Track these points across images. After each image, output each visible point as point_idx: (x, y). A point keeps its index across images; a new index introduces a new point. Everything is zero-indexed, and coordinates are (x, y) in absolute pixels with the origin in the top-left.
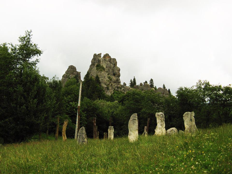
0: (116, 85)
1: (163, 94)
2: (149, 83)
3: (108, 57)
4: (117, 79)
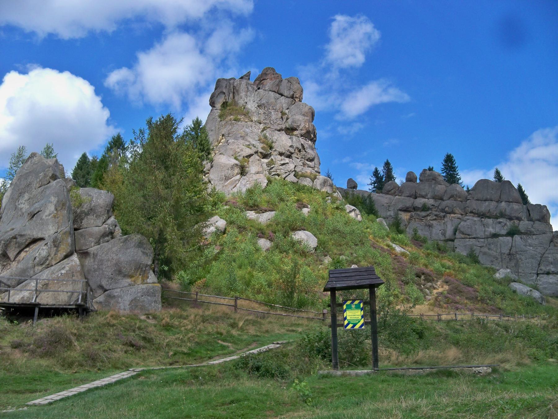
0: (291, 166)
1: (497, 202)
2: (439, 168)
3: (271, 79)
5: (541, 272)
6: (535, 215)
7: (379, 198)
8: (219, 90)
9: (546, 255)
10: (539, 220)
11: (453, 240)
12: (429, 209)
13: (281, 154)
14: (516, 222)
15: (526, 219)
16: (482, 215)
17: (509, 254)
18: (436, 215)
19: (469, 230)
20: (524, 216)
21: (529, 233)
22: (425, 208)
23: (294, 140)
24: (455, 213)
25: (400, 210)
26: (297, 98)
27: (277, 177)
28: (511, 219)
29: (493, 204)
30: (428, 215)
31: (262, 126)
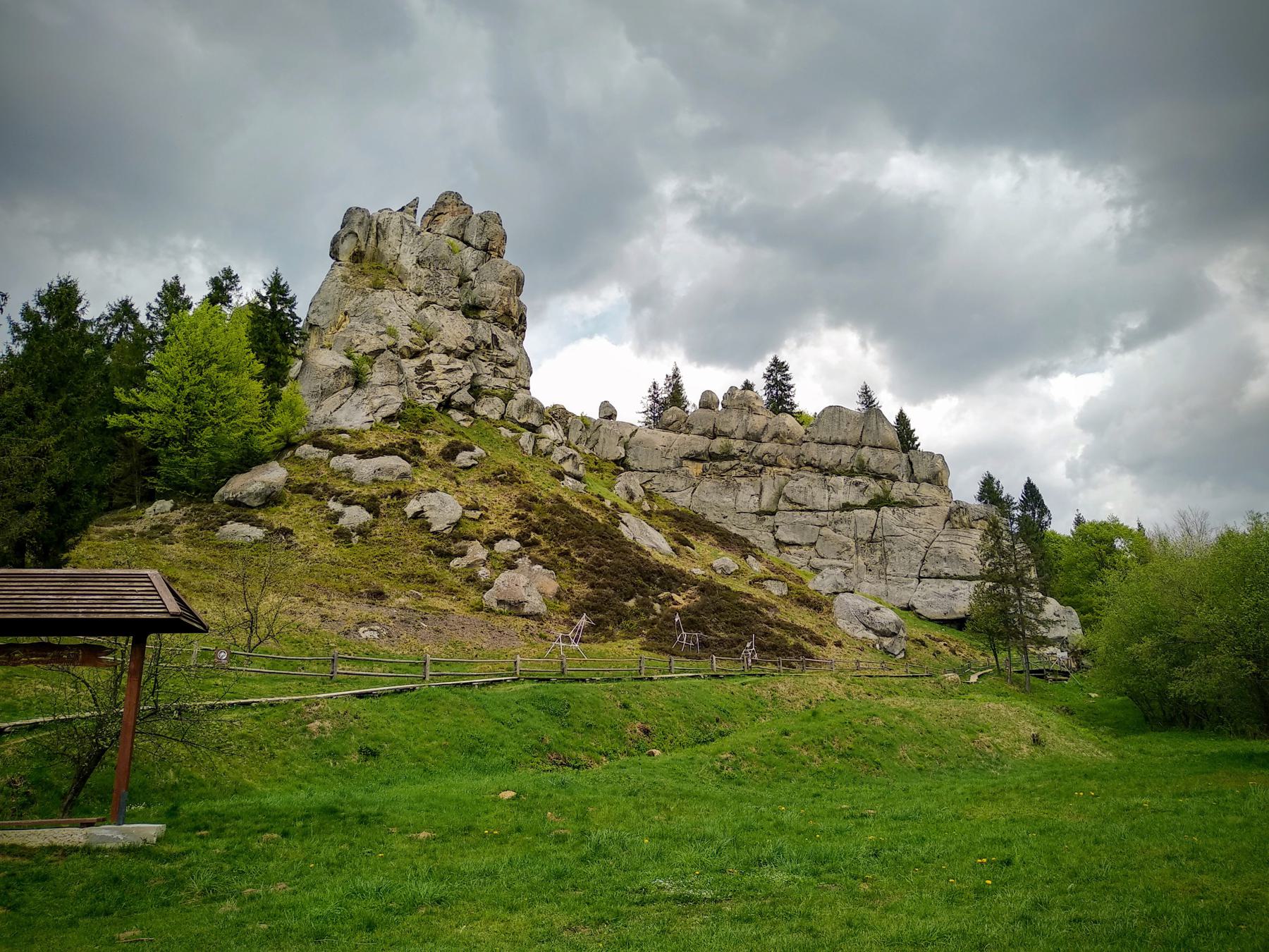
0: (466, 375)
3: (453, 215)
4: (494, 337)
5: (926, 574)
6: (921, 472)
7: (652, 437)
8: (347, 229)
9: (935, 544)
10: (928, 481)
11: (773, 514)
12: (733, 457)
13: (448, 352)
14: (888, 483)
15: (905, 479)
16: (826, 471)
17: (871, 541)
18: (745, 469)
19: (802, 496)
20: (901, 472)
21: (910, 504)
22: (727, 456)
23: (480, 326)
24: (780, 466)
25: (685, 458)
26: (493, 250)
27: (433, 392)
28: (877, 477)
29: (849, 450)
30: (732, 468)
31: (421, 299)
